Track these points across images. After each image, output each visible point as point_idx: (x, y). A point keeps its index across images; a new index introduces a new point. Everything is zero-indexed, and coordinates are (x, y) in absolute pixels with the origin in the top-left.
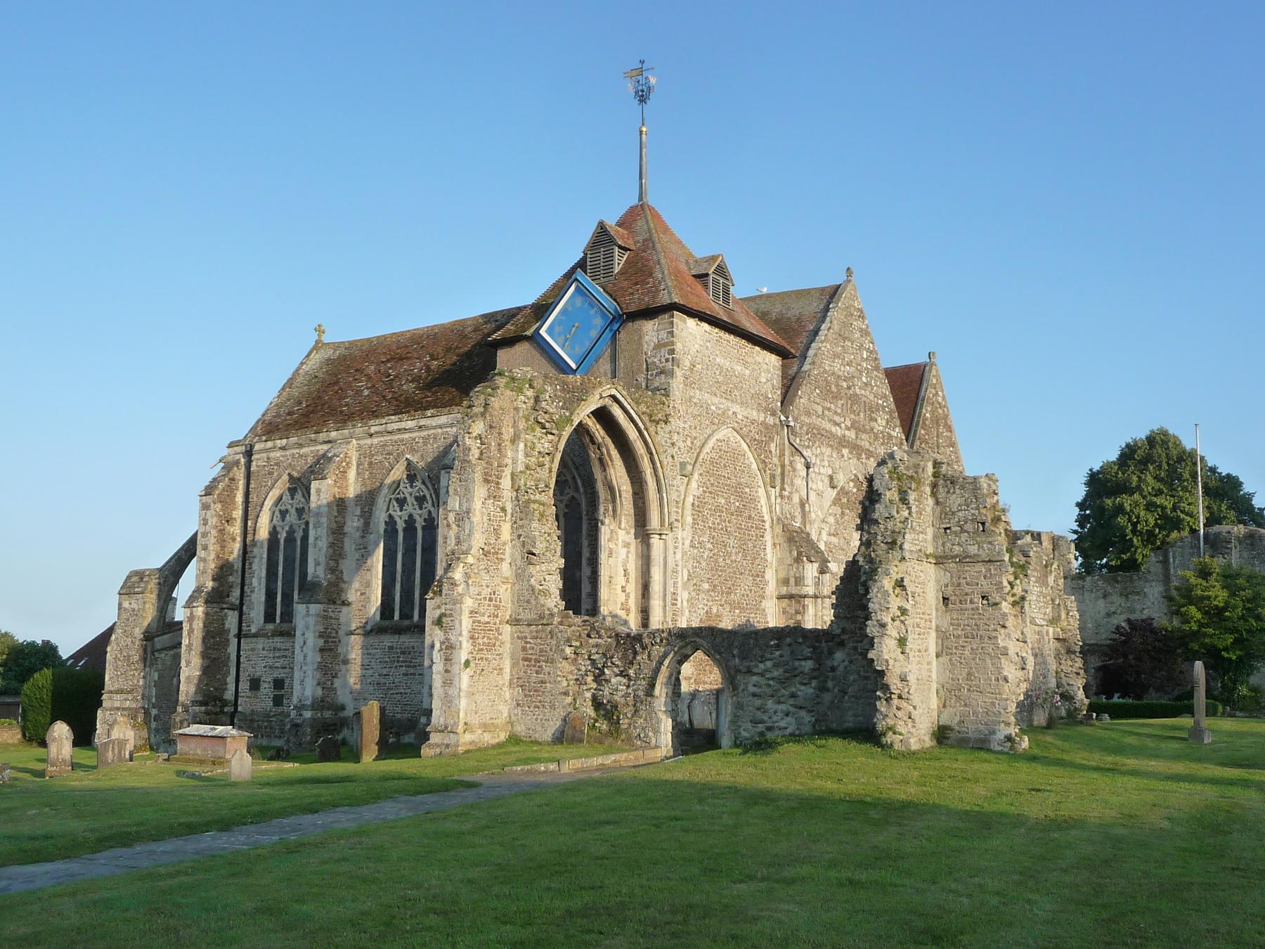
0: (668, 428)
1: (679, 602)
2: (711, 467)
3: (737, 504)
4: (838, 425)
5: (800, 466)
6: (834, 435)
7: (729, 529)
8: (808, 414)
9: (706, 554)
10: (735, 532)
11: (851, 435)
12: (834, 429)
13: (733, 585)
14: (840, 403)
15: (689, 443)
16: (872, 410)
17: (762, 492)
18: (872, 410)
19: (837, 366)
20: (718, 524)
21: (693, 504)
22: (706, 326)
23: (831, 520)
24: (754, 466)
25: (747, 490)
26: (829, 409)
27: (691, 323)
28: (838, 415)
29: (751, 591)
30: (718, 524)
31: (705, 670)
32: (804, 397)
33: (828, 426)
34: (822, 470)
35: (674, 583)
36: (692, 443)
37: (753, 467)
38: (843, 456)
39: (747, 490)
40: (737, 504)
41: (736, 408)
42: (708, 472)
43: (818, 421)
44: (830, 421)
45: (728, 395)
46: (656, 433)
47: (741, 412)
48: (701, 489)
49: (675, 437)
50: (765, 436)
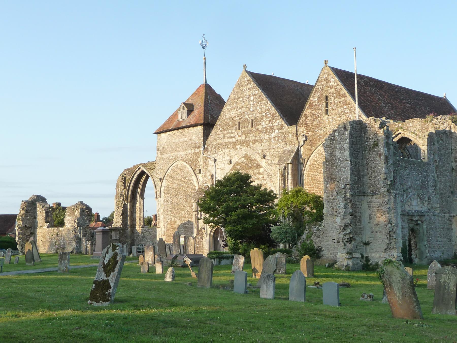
0: (155, 170)
1: (160, 219)
2: (171, 176)
3: (182, 184)
4: (234, 137)
5: (211, 162)
6: (229, 143)
7: (178, 193)
8: (215, 140)
9: (170, 203)
10: (182, 193)
11: (243, 137)
12: (230, 140)
13: (181, 211)
14: (234, 128)
15: (162, 172)
17: (194, 177)
19: (233, 113)
20: (174, 193)
21: (164, 189)
22: (168, 133)
24: (190, 169)
25: (187, 178)
26: (228, 133)
27: (163, 135)
28: (235, 133)
29: (189, 212)
30: (174, 193)
31: (170, 238)
32: (212, 135)
33: (226, 140)
34: (224, 159)
35: (159, 213)
36: (163, 171)
37: (189, 170)
38: (237, 149)
39: (187, 178)
40: (182, 184)
41: (181, 153)
42: (170, 178)
43: (221, 141)
44: (228, 138)
45: (178, 150)
46: (152, 173)
47: (183, 154)
48: (167, 184)
49: (158, 172)
50: (195, 157)
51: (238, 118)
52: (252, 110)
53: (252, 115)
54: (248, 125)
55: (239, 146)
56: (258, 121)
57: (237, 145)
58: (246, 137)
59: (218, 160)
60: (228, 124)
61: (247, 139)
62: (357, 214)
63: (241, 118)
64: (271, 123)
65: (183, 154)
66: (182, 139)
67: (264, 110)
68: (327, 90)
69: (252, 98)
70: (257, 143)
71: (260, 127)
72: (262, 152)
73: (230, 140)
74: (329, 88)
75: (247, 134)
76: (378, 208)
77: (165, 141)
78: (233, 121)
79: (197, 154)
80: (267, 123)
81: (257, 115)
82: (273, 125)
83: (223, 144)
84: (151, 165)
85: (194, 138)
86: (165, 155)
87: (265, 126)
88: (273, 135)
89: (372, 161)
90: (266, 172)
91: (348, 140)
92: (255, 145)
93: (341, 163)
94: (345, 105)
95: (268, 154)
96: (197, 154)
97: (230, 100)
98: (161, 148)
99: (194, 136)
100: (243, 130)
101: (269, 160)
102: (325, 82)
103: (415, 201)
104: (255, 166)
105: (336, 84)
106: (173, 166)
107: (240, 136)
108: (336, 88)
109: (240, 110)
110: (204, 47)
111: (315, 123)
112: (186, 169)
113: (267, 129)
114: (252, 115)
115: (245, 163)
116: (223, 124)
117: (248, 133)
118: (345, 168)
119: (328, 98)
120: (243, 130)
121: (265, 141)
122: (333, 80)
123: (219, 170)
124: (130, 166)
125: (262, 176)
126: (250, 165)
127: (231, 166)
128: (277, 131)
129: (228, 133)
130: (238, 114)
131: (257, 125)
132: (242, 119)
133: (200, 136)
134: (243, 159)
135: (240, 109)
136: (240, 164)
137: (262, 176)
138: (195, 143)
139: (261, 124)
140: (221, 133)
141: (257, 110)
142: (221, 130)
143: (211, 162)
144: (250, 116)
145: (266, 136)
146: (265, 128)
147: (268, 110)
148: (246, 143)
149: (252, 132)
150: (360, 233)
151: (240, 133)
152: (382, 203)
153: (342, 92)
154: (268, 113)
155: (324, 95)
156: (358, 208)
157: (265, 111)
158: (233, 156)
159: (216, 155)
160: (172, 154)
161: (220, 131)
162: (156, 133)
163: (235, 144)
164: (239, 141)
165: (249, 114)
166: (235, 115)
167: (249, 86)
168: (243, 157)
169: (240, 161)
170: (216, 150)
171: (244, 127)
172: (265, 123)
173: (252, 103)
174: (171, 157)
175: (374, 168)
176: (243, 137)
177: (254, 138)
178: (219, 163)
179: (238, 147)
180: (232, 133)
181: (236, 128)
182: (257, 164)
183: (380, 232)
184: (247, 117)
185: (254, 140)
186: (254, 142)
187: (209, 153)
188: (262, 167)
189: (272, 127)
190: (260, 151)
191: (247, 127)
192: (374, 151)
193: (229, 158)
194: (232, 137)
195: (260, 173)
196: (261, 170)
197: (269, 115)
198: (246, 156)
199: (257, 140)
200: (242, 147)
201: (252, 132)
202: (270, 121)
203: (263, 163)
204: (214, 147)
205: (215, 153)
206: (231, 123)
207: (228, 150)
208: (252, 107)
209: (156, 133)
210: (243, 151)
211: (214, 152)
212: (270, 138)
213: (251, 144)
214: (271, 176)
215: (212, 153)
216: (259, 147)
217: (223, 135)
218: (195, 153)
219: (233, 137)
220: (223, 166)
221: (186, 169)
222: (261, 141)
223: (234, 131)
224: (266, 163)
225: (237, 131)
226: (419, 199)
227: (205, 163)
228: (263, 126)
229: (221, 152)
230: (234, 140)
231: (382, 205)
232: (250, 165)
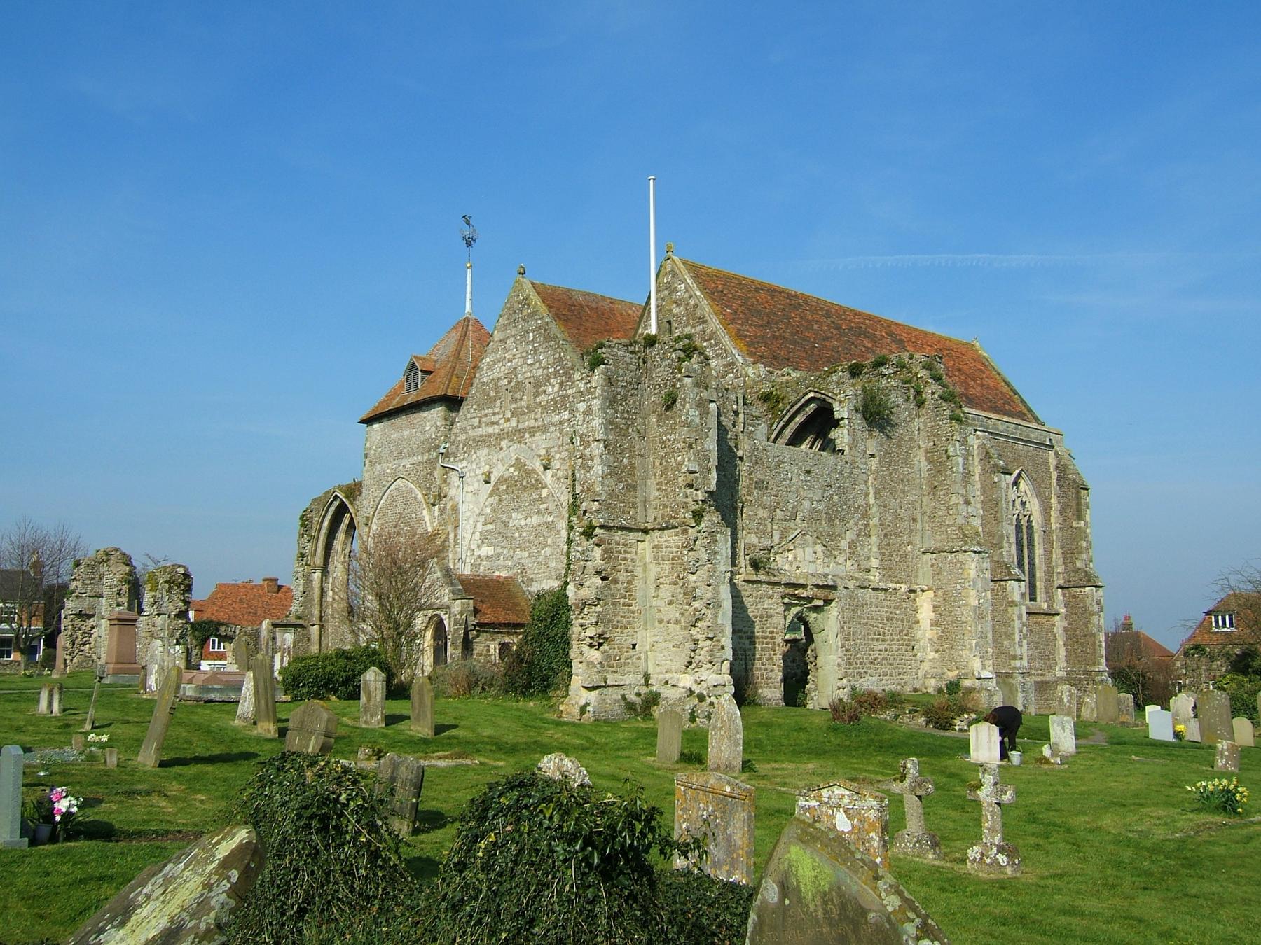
4: (497, 423)
6: (490, 436)
8: (465, 431)
12: (490, 430)
14: (498, 403)
15: (372, 503)
16: (538, 385)
17: (425, 512)
23: (488, 510)
26: (486, 415)
27: (376, 426)
28: (498, 413)
38: (501, 449)
39: (414, 515)
44: (487, 424)
45: (400, 456)
47: (407, 463)
51: (505, 382)
52: (529, 362)
53: (530, 372)
54: (523, 395)
55: (506, 441)
56: (541, 386)
57: (501, 440)
58: (518, 422)
59: (468, 475)
60: (488, 396)
61: (521, 426)
62: (621, 576)
63: (509, 382)
64: (565, 390)
65: (407, 463)
66: (407, 433)
67: (551, 360)
68: (671, 311)
70: (539, 434)
71: (543, 399)
72: (547, 452)
73: (490, 430)
74: (675, 305)
75: (521, 415)
76: (673, 559)
77: (379, 438)
78: (497, 388)
79: (432, 462)
80: (556, 389)
81: (539, 373)
82: (568, 392)
83: (478, 439)
84: (354, 490)
85: (427, 428)
86: (378, 466)
87: (552, 396)
89: (664, 442)
90: (553, 496)
91: (599, 391)
92: (534, 439)
93: (585, 449)
94: (706, 341)
95: (557, 456)
96: (432, 462)
97: (491, 344)
98: (373, 452)
99: (428, 424)
100: (514, 406)
101: (558, 470)
102: (666, 292)
103: (809, 550)
104: (532, 485)
105: (687, 295)
106: (390, 489)
107: (508, 420)
108: (688, 304)
109: (509, 364)
110: (469, 244)
112: (413, 495)
113: (556, 402)
114: (530, 372)
115: (516, 478)
116: (478, 396)
117: (523, 414)
118: (593, 461)
119: (673, 328)
120: (514, 406)
121: (552, 429)
122: (683, 286)
123: (471, 494)
124: (319, 494)
125: (544, 506)
126: (525, 483)
127: (490, 487)
129: (486, 415)
130: (506, 372)
131: (539, 395)
132: (512, 384)
133: (438, 424)
134: (512, 469)
135: (510, 361)
136: (506, 480)
137: (544, 506)
138: (429, 440)
139: (545, 391)
140: (474, 415)
142: (475, 410)
143: (454, 477)
144: (526, 375)
145: (555, 418)
146: (552, 400)
147: (560, 360)
148: (517, 435)
149: (530, 409)
150: (629, 623)
151: (508, 415)
152: (682, 547)
153: (699, 313)
154: (558, 368)
155: (664, 320)
156: (625, 559)
157: (554, 363)
158: (494, 463)
159: (465, 463)
160: (390, 465)
161: (472, 411)
162: (362, 422)
163: (499, 437)
164: (506, 431)
165: (525, 372)
166: (499, 376)
167: (525, 312)
168: (512, 466)
169: (506, 475)
170: (465, 453)
171: (516, 400)
172: (552, 389)
173: (530, 348)
174: (388, 471)
175: (667, 461)
176: (513, 423)
177: (532, 423)
178: (469, 480)
179: (504, 444)
180: (494, 414)
181: (501, 403)
182: (537, 480)
183: (677, 622)
184: (520, 378)
186: (533, 431)
187: (452, 459)
188: (546, 487)
190: (543, 452)
191: (521, 399)
192: (667, 419)
193: (487, 468)
194: (493, 423)
195: (541, 500)
196: (545, 493)
197: (561, 372)
198: (519, 465)
199: (538, 427)
200: (511, 444)
201: (530, 412)
202: (561, 384)
203: (548, 478)
204: (461, 446)
205: (463, 459)
206: (492, 394)
207: (486, 451)
208: (530, 356)
209: (362, 422)
210: (512, 451)
211: (462, 457)
213: (527, 436)
214: (562, 504)
215: (458, 459)
216: (540, 443)
217: (477, 419)
218: (429, 461)
219: (493, 423)
220: (476, 485)
221: (413, 495)
222: (544, 429)
223: (497, 410)
224: (552, 477)
225: (503, 409)
226: (819, 548)
227: (445, 481)
228: (549, 395)
229: (474, 457)
230: (496, 429)
231: (681, 553)
232: (525, 483)
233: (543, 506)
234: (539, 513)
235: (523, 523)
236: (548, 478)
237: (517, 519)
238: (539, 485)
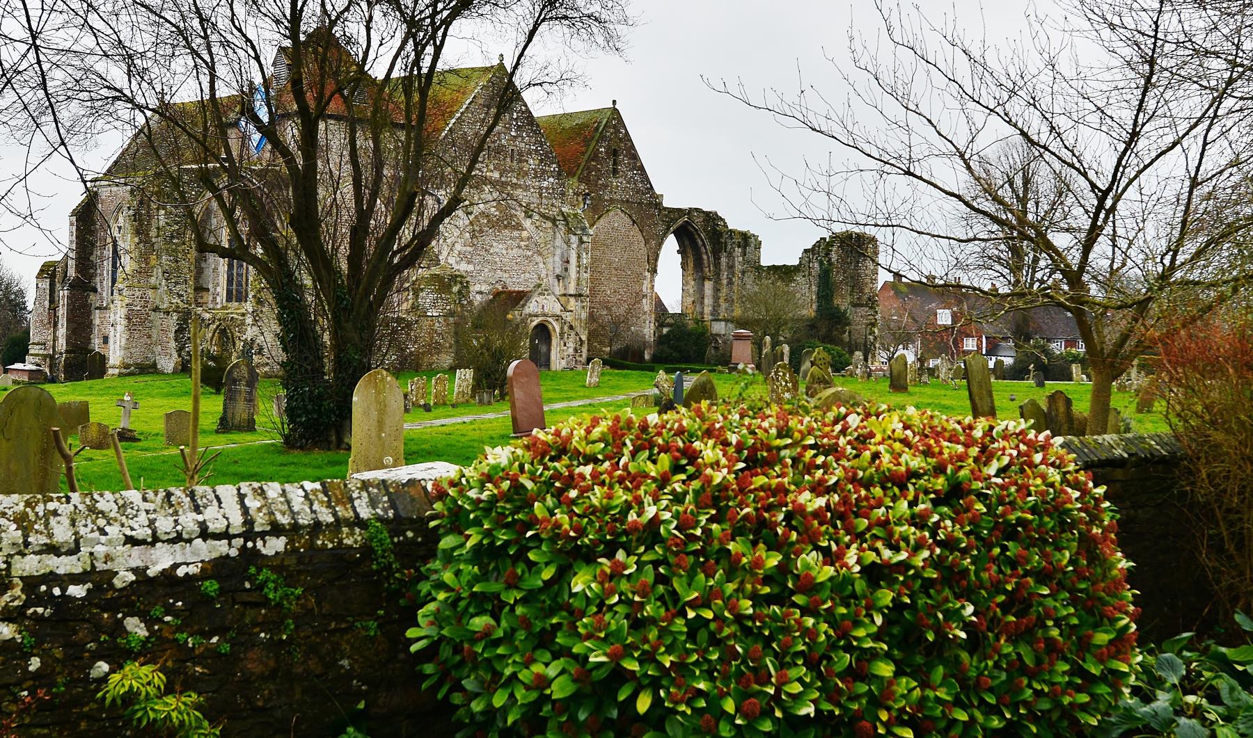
16: (521, 157)
18: (521, 157)
52: (513, 134)
58: (501, 176)
61: (503, 179)
69: (515, 116)
80: (537, 162)
88: (545, 184)
111: (600, 182)
117: (505, 170)
128: (551, 180)
141: (523, 138)
151: (492, 167)
176: (496, 175)
177: (515, 181)
185: (516, 184)
189: (544, 172)
196: (525, 234)
202: (541, 161)
203: (527, 223)
212: (541, 188)
222: (526, 188)
232: (506, 223)
233: (522, 244)
234: (519, 247)
235: (504, 252)
236: (527, 223)
237: (498, 248)
238: (519, 227)
